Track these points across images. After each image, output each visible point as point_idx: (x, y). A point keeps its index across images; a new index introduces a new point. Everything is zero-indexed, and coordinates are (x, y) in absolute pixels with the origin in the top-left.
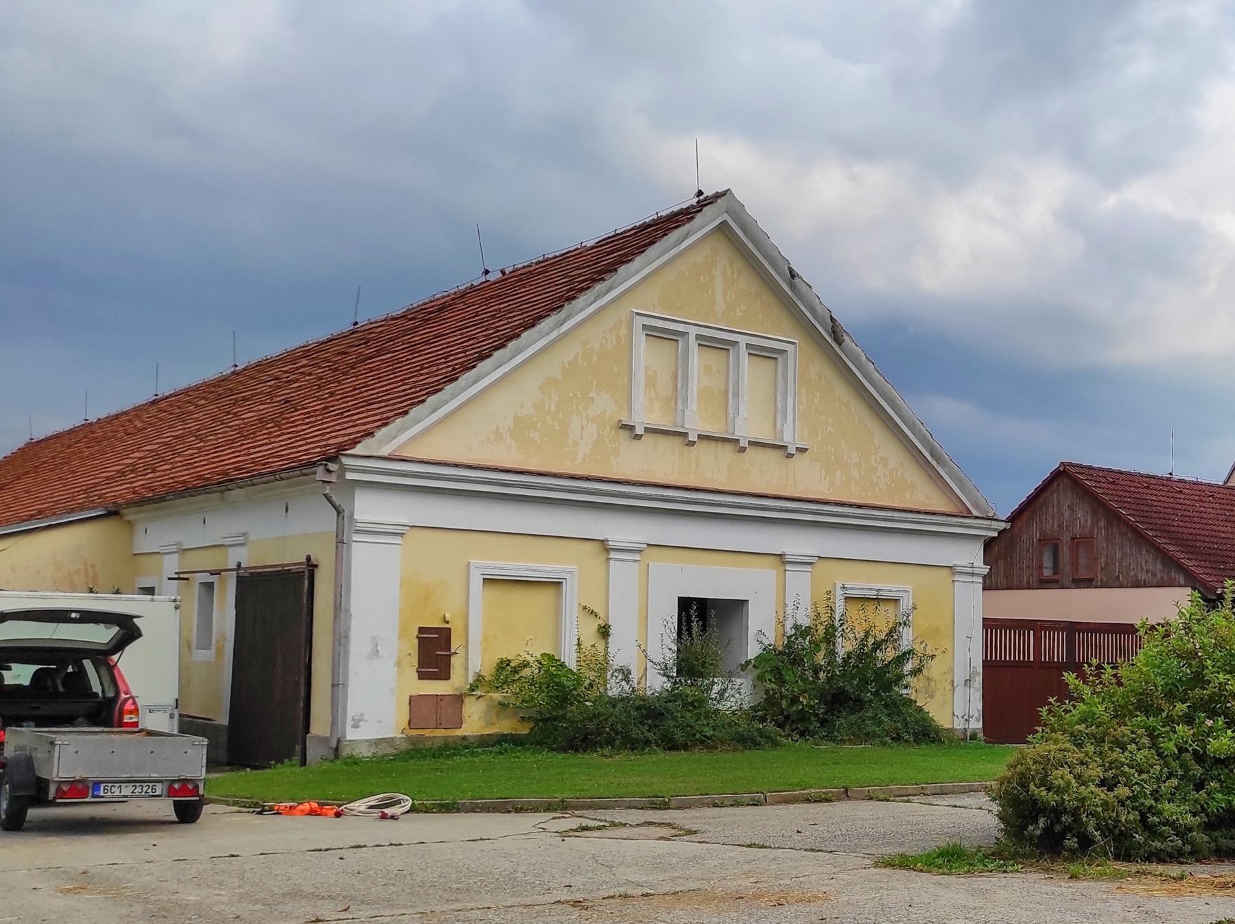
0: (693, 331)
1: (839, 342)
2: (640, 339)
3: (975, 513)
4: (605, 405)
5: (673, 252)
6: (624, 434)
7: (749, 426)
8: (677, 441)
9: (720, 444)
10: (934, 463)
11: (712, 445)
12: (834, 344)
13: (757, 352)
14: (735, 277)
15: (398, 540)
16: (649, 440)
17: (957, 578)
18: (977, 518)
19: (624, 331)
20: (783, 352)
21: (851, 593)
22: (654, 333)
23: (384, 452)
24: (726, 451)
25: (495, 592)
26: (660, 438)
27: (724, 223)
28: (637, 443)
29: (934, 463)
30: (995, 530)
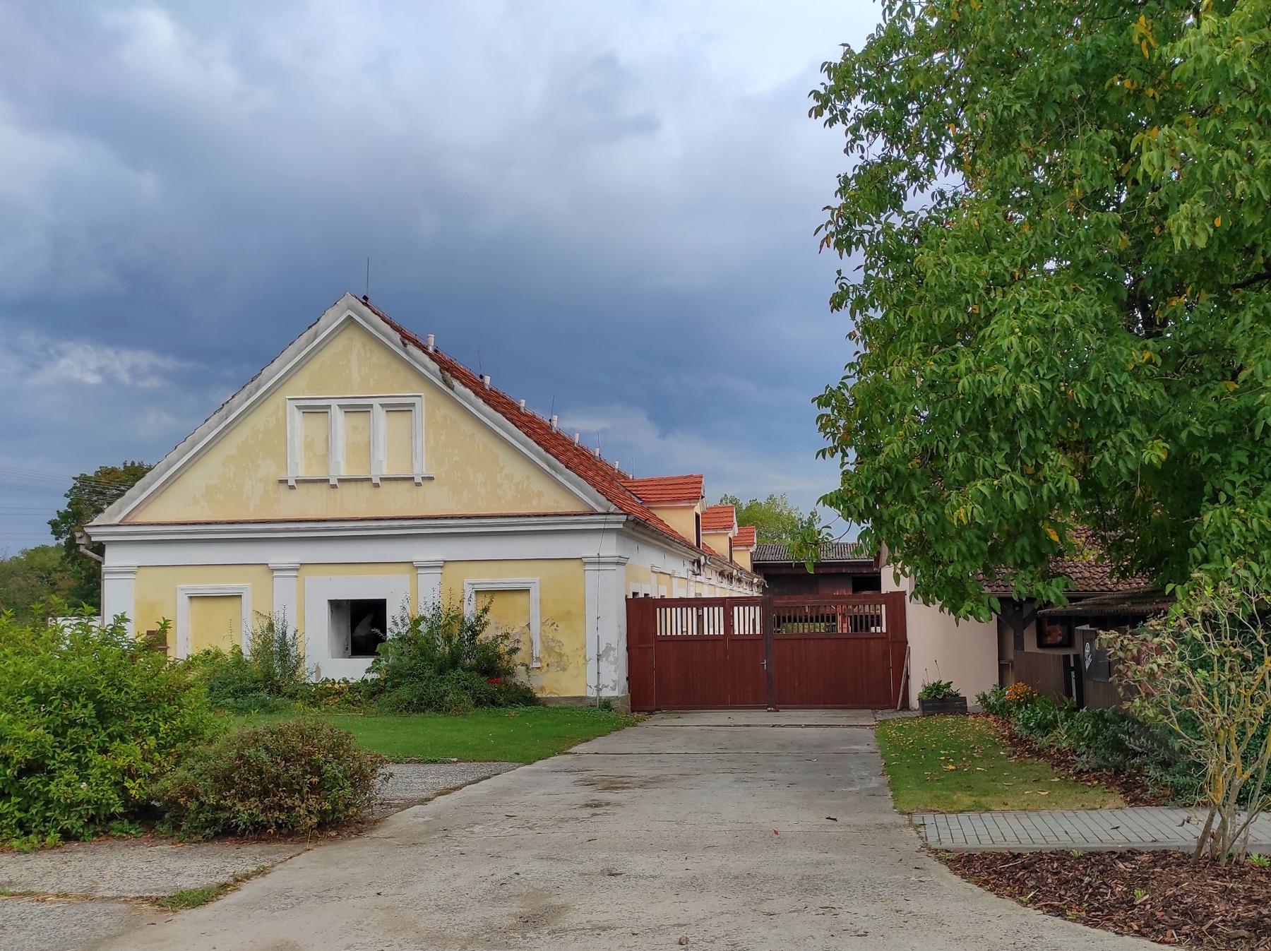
0: (376, 402)
1: (452, 388)
2: (298, 415)
3: (600, 510)
4: (269, 469)
5: (308, 349)
6: (283, 487)
7: (383, 466)
8: (324, 486)
9: (359, 484)
10: (553, 472)
11: (353, 486)
12: (449, 391)
13: (391, 409)
14: (368, 355)
15: (132, 576)
16: (302, 489)
17: (587, 567)
18: (599, 514)
19: (281, 413)
20: (413, 405)
21: (479, 587)
22: (308, 410)
23: (116, 521)
24: (365, 489)
25: (198, 605)
26: (312, 487)
27: (350, 317)
28: (293, 492)
29: (553, 472)
30: (619, 523)
